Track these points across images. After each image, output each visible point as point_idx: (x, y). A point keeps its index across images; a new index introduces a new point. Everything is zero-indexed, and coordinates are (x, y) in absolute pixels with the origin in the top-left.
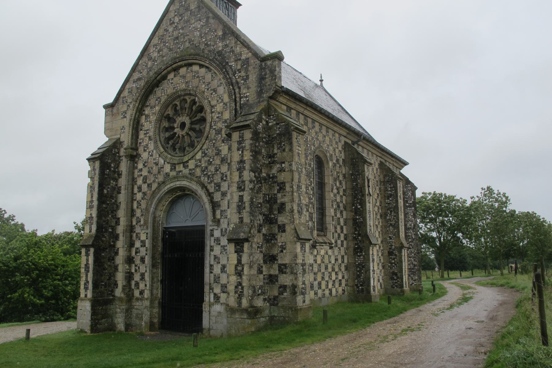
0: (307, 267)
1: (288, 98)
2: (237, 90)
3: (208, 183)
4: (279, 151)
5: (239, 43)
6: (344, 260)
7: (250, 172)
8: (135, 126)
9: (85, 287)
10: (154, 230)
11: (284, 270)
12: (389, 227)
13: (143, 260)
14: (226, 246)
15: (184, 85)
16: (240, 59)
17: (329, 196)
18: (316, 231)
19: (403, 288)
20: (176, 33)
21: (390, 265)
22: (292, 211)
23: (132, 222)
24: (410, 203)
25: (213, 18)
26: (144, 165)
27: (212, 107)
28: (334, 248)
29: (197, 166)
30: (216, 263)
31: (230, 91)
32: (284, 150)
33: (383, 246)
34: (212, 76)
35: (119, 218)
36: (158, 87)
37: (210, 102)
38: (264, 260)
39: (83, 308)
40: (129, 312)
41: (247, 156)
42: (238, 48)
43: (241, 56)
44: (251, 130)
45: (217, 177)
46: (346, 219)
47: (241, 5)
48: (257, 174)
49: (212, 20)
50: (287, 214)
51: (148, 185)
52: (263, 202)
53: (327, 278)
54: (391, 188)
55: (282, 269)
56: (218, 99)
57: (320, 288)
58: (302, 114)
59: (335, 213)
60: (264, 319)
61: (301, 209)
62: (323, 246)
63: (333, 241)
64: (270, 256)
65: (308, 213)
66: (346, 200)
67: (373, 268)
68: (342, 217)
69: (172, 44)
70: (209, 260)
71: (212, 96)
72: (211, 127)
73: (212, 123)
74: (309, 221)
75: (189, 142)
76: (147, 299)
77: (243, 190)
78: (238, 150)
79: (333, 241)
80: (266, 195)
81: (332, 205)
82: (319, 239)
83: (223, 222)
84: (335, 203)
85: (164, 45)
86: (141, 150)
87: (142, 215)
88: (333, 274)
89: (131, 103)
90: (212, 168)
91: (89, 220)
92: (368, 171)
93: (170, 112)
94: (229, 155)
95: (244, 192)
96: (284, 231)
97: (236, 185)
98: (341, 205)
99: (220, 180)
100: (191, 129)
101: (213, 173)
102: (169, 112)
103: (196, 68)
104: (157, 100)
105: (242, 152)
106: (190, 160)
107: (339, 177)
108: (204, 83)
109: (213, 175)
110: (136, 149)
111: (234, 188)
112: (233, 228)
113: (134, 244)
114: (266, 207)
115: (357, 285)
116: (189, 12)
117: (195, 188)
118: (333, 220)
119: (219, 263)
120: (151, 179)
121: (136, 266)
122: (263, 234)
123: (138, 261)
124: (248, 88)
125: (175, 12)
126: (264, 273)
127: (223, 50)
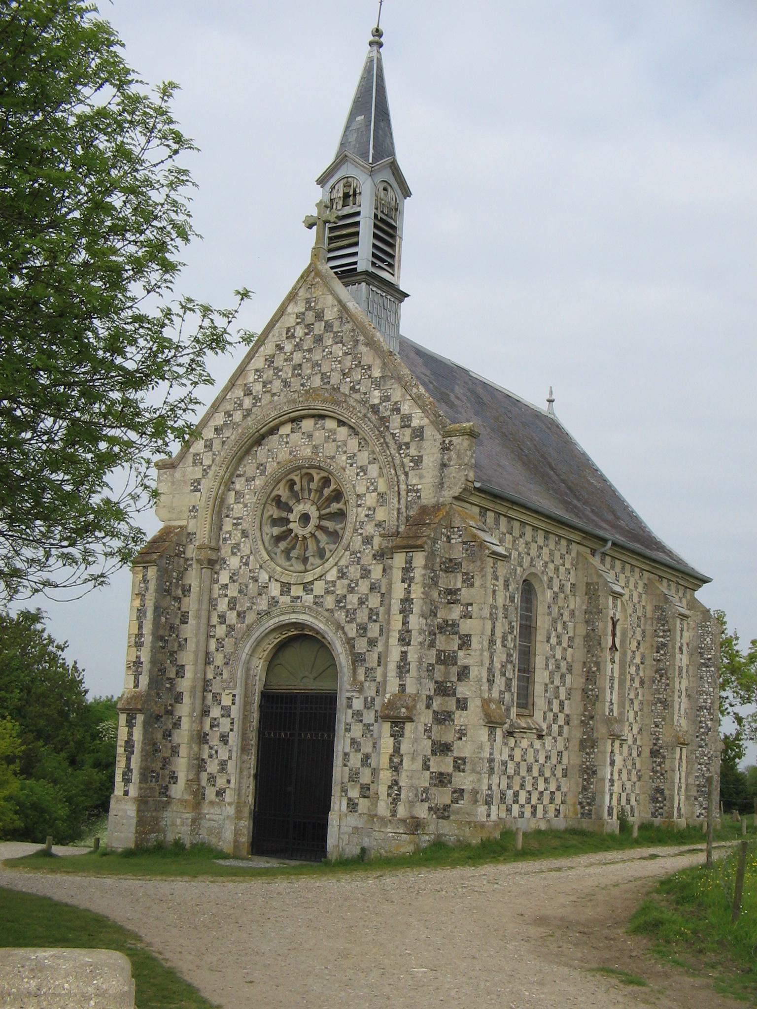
0: (496, 765)
2: (402, 477)
5: (408, 397)
6: (561, 759)
7: (419, 618)
8: (216, 509)
10: (246, 689)
11: (462, 767)
12: (656, 704)
13: (224, 739)
16: (409, 426)
17: (541, 649)
18: (515, 708)
19: (673, 818)
20: (298, 357)
21: (652, 774)
22: (479, 680)
23: (205, 674)
24: (709, 659)
25: (367, 345)
26: (231, 578)
28: (545, 737)
29: (327, 592)
31: (390, 477)
32: (472, 585)
33: (641, 739)
34: (360, 443)
35: (183, 666)
36: (260, 445)
37: (354, 486)
38: (432, 750)
39: (120, 814)
40: (197, 823)
41: (417, 592)
42: (406, 407)
43: (411, 420)
44: (424, 553)
45: (361, 614)
46: (570, 689)
48: (429, 621)
49: (363, 347)
50: (472, 683)
51: (239, 614)
52: (437, 663)
53: (529, 787)
54: (664, 631)
55: (459, 764)
56: (369, 484)
57: (516, 801)
58: (503, 515)
59: (550, 679)
60: (427, 837)
61: (494, 676)
62: (525, 733)
63: (544, 727)
64: (441, 745)
65: (504, 678)
66: (573, 656)
67: (612, 775)
68: (564, 685)
69: (290, 375)
70: (341, 745)
71: (359, 477)
72: (355, 530)
74: (504, 692)
76: (230, 804)
77: (409, 644)
78: (403, 581)
79: (544, 727)
80: (442, 651)
81: (547, 665)
82: (519, 721)
83: (369, 687)
84: (552, 662)
85: (276, 374)
86: (226, 552)
87: (226, 664)
88: (541, 781)
89: (209, 467)
90: (353, 599)
91: (134, 666)
92: (615, 606)
93: (282, 491)
94: (384, 582)
95: (409, 647)
97: (398, 635)
98: (563, 665)
99: (366, 619)
100: (319, 527)
101: (356, 606)
102: (280, 493)
103: (331, 424)
104: (258, 468)
105: (409, 586)
106: (316, 579)
108: (345, 452)
110: (217, 549)
111: (394, 640)
112: (389, 700)
113: (209, 711)
114: (439, 670)
115: (580, 803)
116: (323, 324)
117: (323, 628)
118: (546, 691)
121: (211, 748)
122: (434, 711)
123: (214, 741)
124: (421, 477)
127: (380, 403)
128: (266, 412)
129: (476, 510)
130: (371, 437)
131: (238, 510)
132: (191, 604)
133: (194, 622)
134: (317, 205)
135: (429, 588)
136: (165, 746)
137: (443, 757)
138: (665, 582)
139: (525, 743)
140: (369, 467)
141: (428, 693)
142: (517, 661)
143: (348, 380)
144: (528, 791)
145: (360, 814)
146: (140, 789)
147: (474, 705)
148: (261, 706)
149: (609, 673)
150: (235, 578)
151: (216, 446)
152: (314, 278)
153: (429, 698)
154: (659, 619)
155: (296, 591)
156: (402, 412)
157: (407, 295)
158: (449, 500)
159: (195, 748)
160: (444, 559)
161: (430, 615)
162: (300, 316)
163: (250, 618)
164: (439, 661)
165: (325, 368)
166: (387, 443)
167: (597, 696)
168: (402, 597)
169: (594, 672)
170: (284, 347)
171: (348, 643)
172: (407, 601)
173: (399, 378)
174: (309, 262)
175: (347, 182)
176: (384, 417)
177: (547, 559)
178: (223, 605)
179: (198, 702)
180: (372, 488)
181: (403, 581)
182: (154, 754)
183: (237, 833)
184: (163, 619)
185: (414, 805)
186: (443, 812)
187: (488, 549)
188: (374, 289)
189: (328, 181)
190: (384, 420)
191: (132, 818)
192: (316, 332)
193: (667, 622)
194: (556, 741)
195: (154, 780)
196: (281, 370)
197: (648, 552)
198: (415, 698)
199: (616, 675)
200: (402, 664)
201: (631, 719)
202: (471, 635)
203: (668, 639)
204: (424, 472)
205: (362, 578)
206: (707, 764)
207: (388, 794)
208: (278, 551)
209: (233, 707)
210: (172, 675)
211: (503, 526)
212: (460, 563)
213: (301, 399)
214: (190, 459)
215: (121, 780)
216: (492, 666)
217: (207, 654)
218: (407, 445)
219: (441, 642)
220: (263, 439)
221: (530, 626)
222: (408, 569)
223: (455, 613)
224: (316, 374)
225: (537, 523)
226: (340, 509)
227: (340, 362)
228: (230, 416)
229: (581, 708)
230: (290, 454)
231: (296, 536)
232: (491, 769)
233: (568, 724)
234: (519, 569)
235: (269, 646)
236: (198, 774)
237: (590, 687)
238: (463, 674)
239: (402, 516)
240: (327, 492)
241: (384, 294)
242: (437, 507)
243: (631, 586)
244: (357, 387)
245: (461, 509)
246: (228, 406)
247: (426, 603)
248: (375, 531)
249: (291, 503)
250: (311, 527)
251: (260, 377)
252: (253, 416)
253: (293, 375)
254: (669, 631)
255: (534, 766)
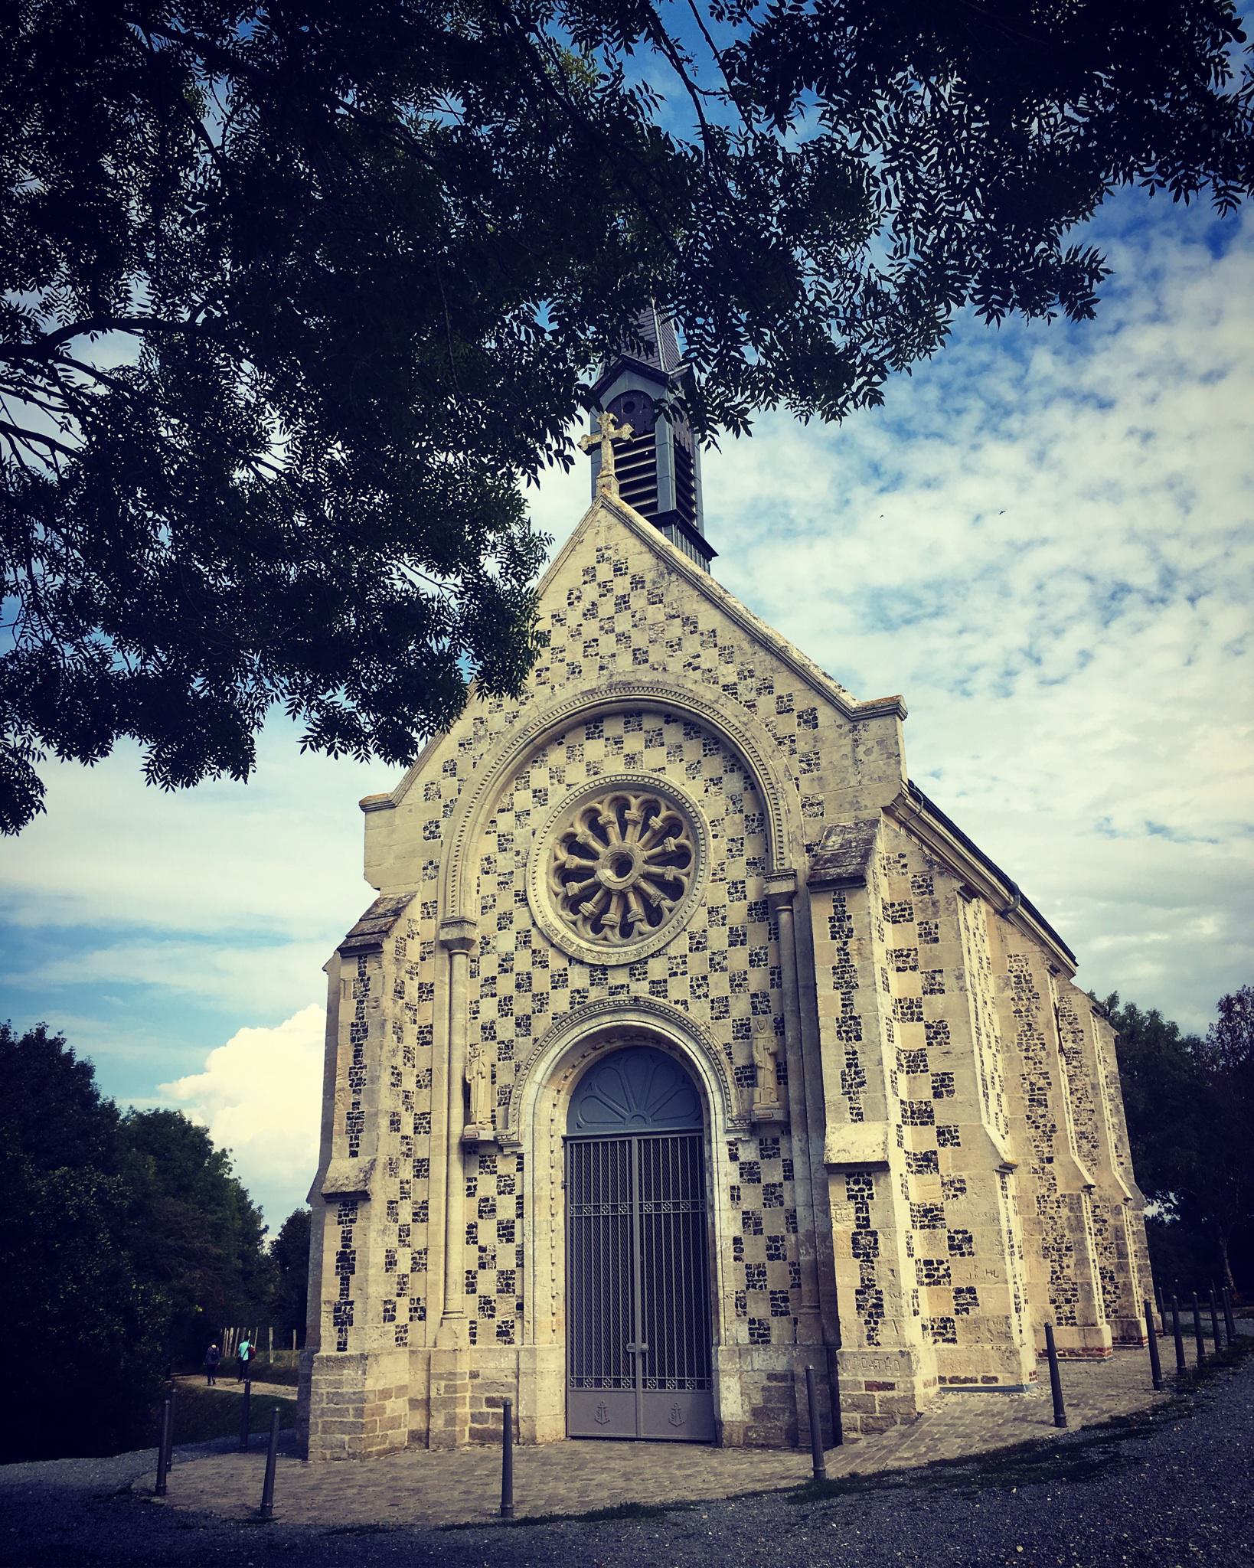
47: (716, 555)
106: (652, 956)
115: (1053, 1302)
119: (758, 1231)
120: (523, 1004)
121: (482, 1249)
163: (542, 1024)
178: (489, 1009)
192: (619, 591)
207: (859, 1307)
226: (680, 847)
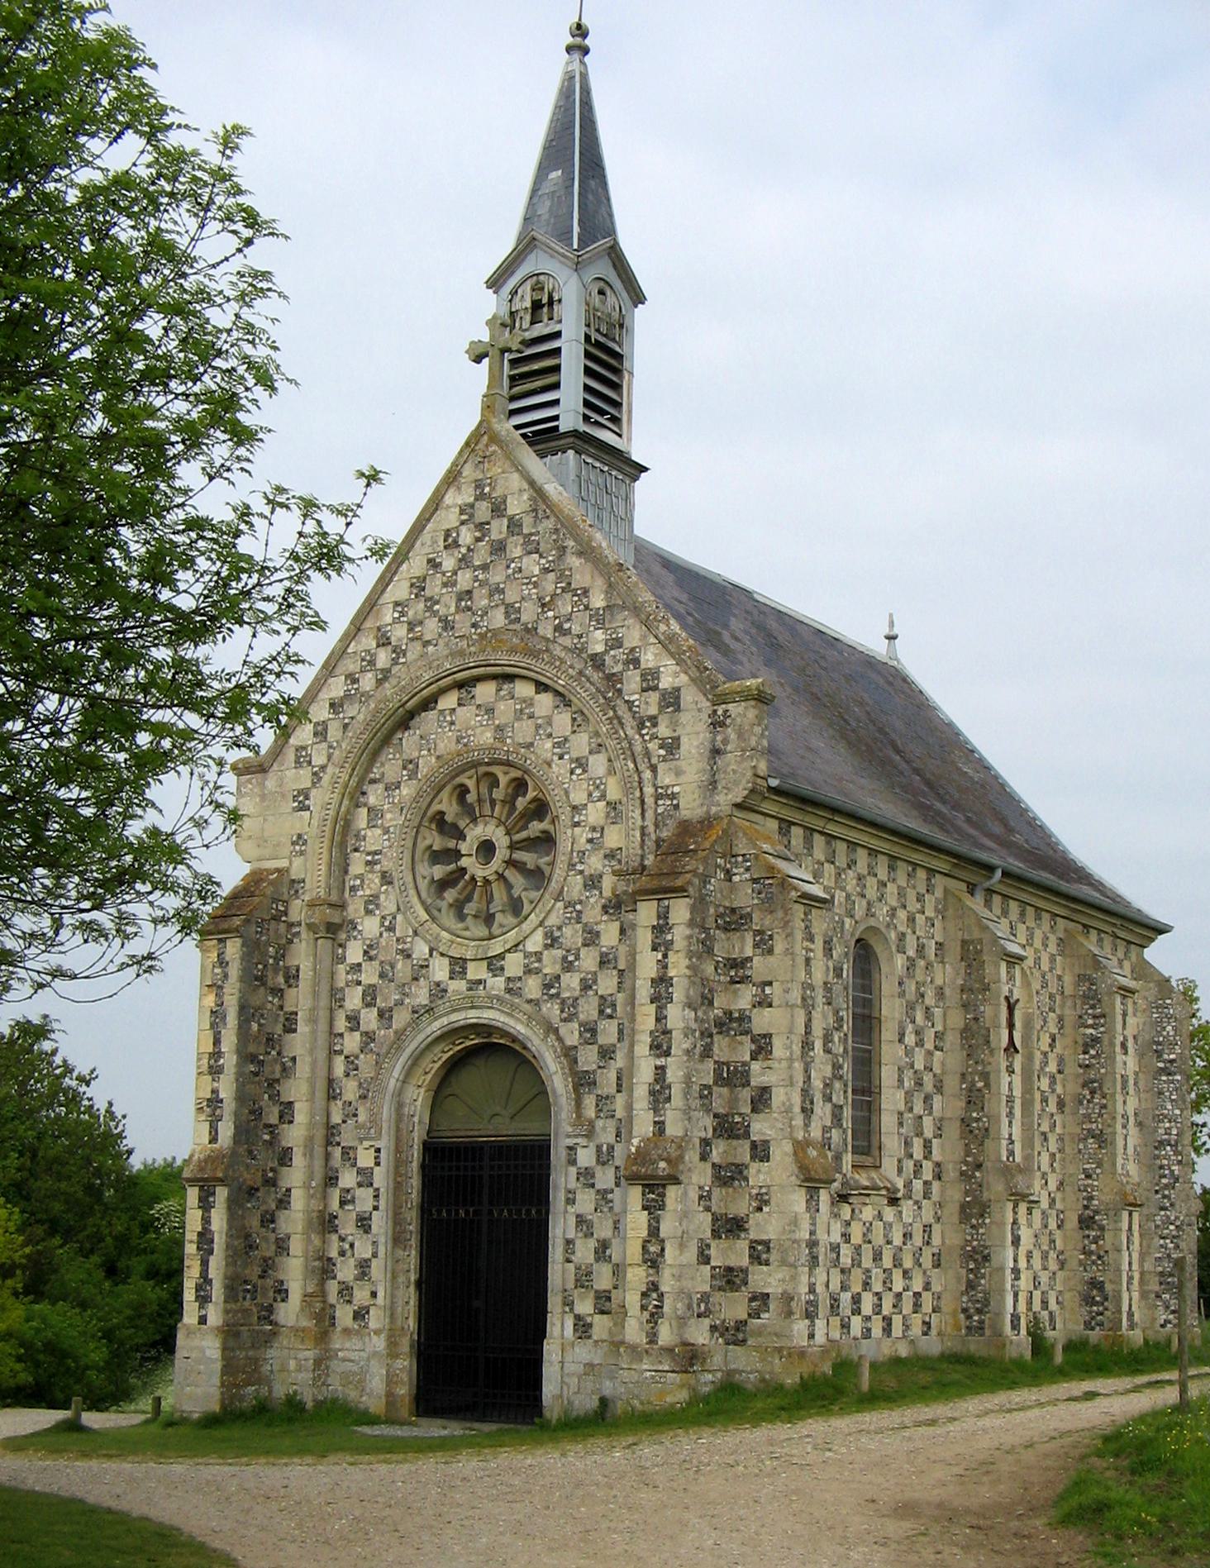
0: (821, 1250)
1: (785, 801)
2: (647, 775)
3: (561, 1020)
4: (758, 951)
6: (929, 1237)
9: (197, 1297)
10: (398, 1140)
11: (764, 1256)
13: (364, 1223)
14: (612, 1191)
15: (489, 735)
16: (655, 688)
17: (890, 1054)
18: (850, 1154)
20: (464, 579)
21: (1082, 1257)
23: (328, 1116)
24: (1172, 1061)
25: (580, 554)
26: (366, 953)
27: (575, 809)
28: (902, 1202)
29: (528, 971)
30: (580, 1235)
31: (627, 774)
32: (770, 951)
33: (1063, 1199)
34: (574, 720)
36: (407, 728)
37: (567, 793)
39: (193, 1355)
41: (678, 966)
42: (650, 656)
43: (658, 678)
44: (687, 900)
46: (941, 1119)
48: (700, 1014)
49: (574, 559)
51: (381, 1014)
52: (716, 1083)
53: (877, 1287)
54: (1095, 1017)
55: (759, 1252)
56: (591, 788)
57: (857, 1311)
58: (821, 833)
59: (906, 1103)
60: (710, 1376)
61: (812, 1103)
62: (868, 1195)
63: (900, 1184)
64: (728, 1220)
65: (829, 1106)
66: (943, 1064)
67: (1015, 1261)
68: (930, 1114)
69: (453, 610)
70: (561, 1227)
71: (574, 777)
72: (572, 866)
73: (575, 854)
74: (831, 1128)
75: (505, 899)
76: (377, 1332)
77: (667, 1054)
78: (654, 949)
79: (900, 1184)
80: (723, 1063)
81: (901, 1081)
82: (857, 1176)
83: (604, 1128)
84: (908, 1076)
85: (429, 609)
86: (356, 910)
87: (364, 1097)
88: (897, 1276)
89: (323, 768)
90: (571, 982)
91: (208, 1106)
92: (1011, 978)
93: (447, 805)
94: (623, 950)
95: (669, 1059)
96: (766, 1158)
98: (928, 1079)
99: (595, 1014)
100: (510, 863)
101: (577, 993)
102: (443, 807)
103: (524, 689)
104: (404, 768)
105: (665, 956)
106: (508, 951)
107: (922, 996)
108: (550, 736)
109: (577, 999)
110: (342, 906)
111: (642, 1048)
112: (638, 1148)
113: (337, 1178)
115: (965, 1310)
116: (505, 521)
117: (523, 1031)
118: (901, 1124)
121: (342, 1239)
122: (714, 1165)
123: (348, 1227)
124: (678, 773)
125: (462, 512)
126: (713, 1263)
127: (606, 651)
128: (415, 671)
129: (773, 825)
130: (593, 708)
131: (374, 839)
132: (300, 999)
133: (307, 1029)
134: (488, 323)
135: (699, 958)
136: (265, 1239)
137: (731, 1241)
138: (1094, 934)
139: (868, 1213)
140: (591, 759)
141: (703, 1135)
142: (850, 1075)
143: (550, 614)
144: (877, 1294)
145: (596, 1342)
146: (227, 1312)
147: (781, 1152)
148: (423, 1167)
149: (1005, 1090)
150: (373, 953)
151: (334, 732)
152: (487, 446)
153: (706, 1143)
154: (1084, 996)
155: (476, 971)
156: (643, 666)
157: (646, 469)
158: (727, 809)
159: (316, 1240)
160: (721, 910)
161: (703, 1004)
162: (467, 510)
163: (401, 1018)
164: (719, 1080)
165: (511, 596)
166: (619, 718)
167: (987, 1130)
168: (654, 975)
169: (979, 1090)
170: (441, 563)
171: (566, 1056)
172: (662, 981)
173: (635, 608)
174: (478, 419)
175: (538, 282)
176: (614, 674)
177: (894, 903)
178: (354, 999)
179: (318, 1163)
180: (596, 794)
181: (654, 949)
182: (247, 1253)
183: (390, 1380)
184: (255, 1026)
185: (685, 1324)
186: (734, 1334)
187: (796, 889)
188: (589, 460)
189: (505, 282)
190: (613, 680)
191: (213, 1361)
192: (495, 536)
193: (1099, 1001)
194: (919, 1208)
195: (248, 1296)
196: (437, 602)
197: (1064, 886)
198: (682, 1143)
199: (1017, 1093)
200: (658, 1087)
201: (1045, 1167)
202: (771, 1035)
203: (1102, 1029)
204: (683, 764)
205: (585, 945)
206: (1174, 1237)
208: (444, 905)
209: (377, 1169)
210: (273, 1119)
211: (819, 853)
212: (750, 915)
213: (473, 649)
214: (290, 755)
215: (193, 1298)
216: (809, 1086)
217: (331, 1082)
218: (654, 720)
219: (722, 1048)
220: (412, 718)
221: (870, 1017)
222: (661, 927)
223: (744, 999)
224: (497, 606)
225: (875, 843)
226: (544, 832)
227: (536, 585)
228: (355, 681)
229: (959, 1152)
230: (458, 742)
231: (473, 878)
232: (813, 1257)
233: (940, 1179)
234: (847, 921)
235: (434, 1063)
236: (322, 1283)
237: (975, 1115)
238: (761, 1100)
239: (650, 840)
240: (521, 803)
241: (606, 468)
242: (707, 823)
243: (1038, 943)
244: (566, 626)
245: (748, 824)
246: (351, 665)
247: (694, 983)
248: (604, 866)
249: (462, 824)
250: (496, 863)
251: (403, 614)
252: (393, 681)
253: (458, 610)
254: (1104, 1016)
255: (884, 1251)
